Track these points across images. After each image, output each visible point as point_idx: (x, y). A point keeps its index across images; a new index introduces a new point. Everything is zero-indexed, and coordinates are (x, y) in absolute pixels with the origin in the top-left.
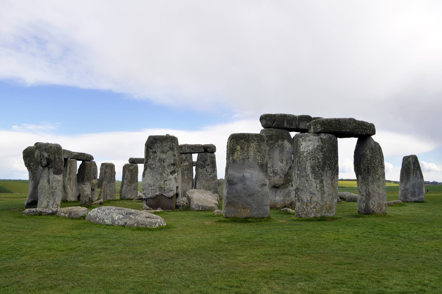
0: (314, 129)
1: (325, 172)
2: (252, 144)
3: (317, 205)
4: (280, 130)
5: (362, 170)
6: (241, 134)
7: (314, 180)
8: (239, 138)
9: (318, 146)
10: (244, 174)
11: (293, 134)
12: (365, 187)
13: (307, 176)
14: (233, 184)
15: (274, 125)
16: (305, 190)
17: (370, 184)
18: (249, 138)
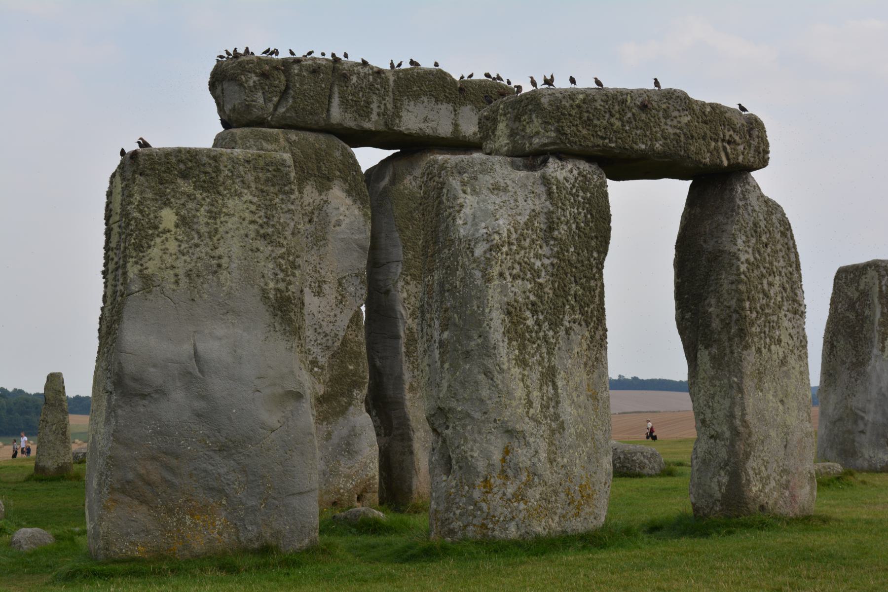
0: (512, 134)
1: (562, 333)
2: (231, 203)
3: (529, 484)
4: (311, 137)
5: (716, 324)
6: (179, 150)
7: (516, 371)
8: (168, 171)
9: (534, 215)
10: (201, 347)
11: (368, 157)
12: (727, 403)
13: (487, 349)
14: (143, 396)
15: (282, 110)
16: (477, 415)
17: (749, 384)
18: (217, 170)
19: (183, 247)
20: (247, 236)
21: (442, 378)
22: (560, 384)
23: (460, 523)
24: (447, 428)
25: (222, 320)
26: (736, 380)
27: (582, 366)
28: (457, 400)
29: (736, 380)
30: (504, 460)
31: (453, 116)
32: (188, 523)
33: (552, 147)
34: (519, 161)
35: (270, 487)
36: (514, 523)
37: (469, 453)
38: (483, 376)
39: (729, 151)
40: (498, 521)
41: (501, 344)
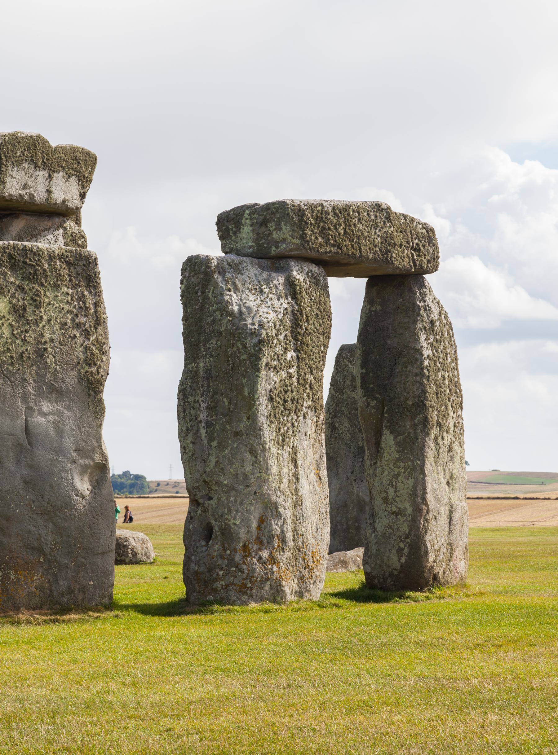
1: (301, 418)
12: (411, 482)
13: (255, 430)
19: (15, 332)
20: (66, 324)
21: (209, 455)
22: (300, 462)
23: (223, 583)
24: (210, 498)
25: (48, 397)
26: (419, 462)
27: (312, 447)
28: (224, 475)
29: (419, 462)
30: (259, 528)
31: (47, 182)
32: (12, 577)
33: (296, 252)
34: (264, 262)
35: (80, 547)
36: (269, 583)
37: (232, 521)
38: (249, 454)
39: (415, 257)
40: (256, 581)
41: (265, 426)
